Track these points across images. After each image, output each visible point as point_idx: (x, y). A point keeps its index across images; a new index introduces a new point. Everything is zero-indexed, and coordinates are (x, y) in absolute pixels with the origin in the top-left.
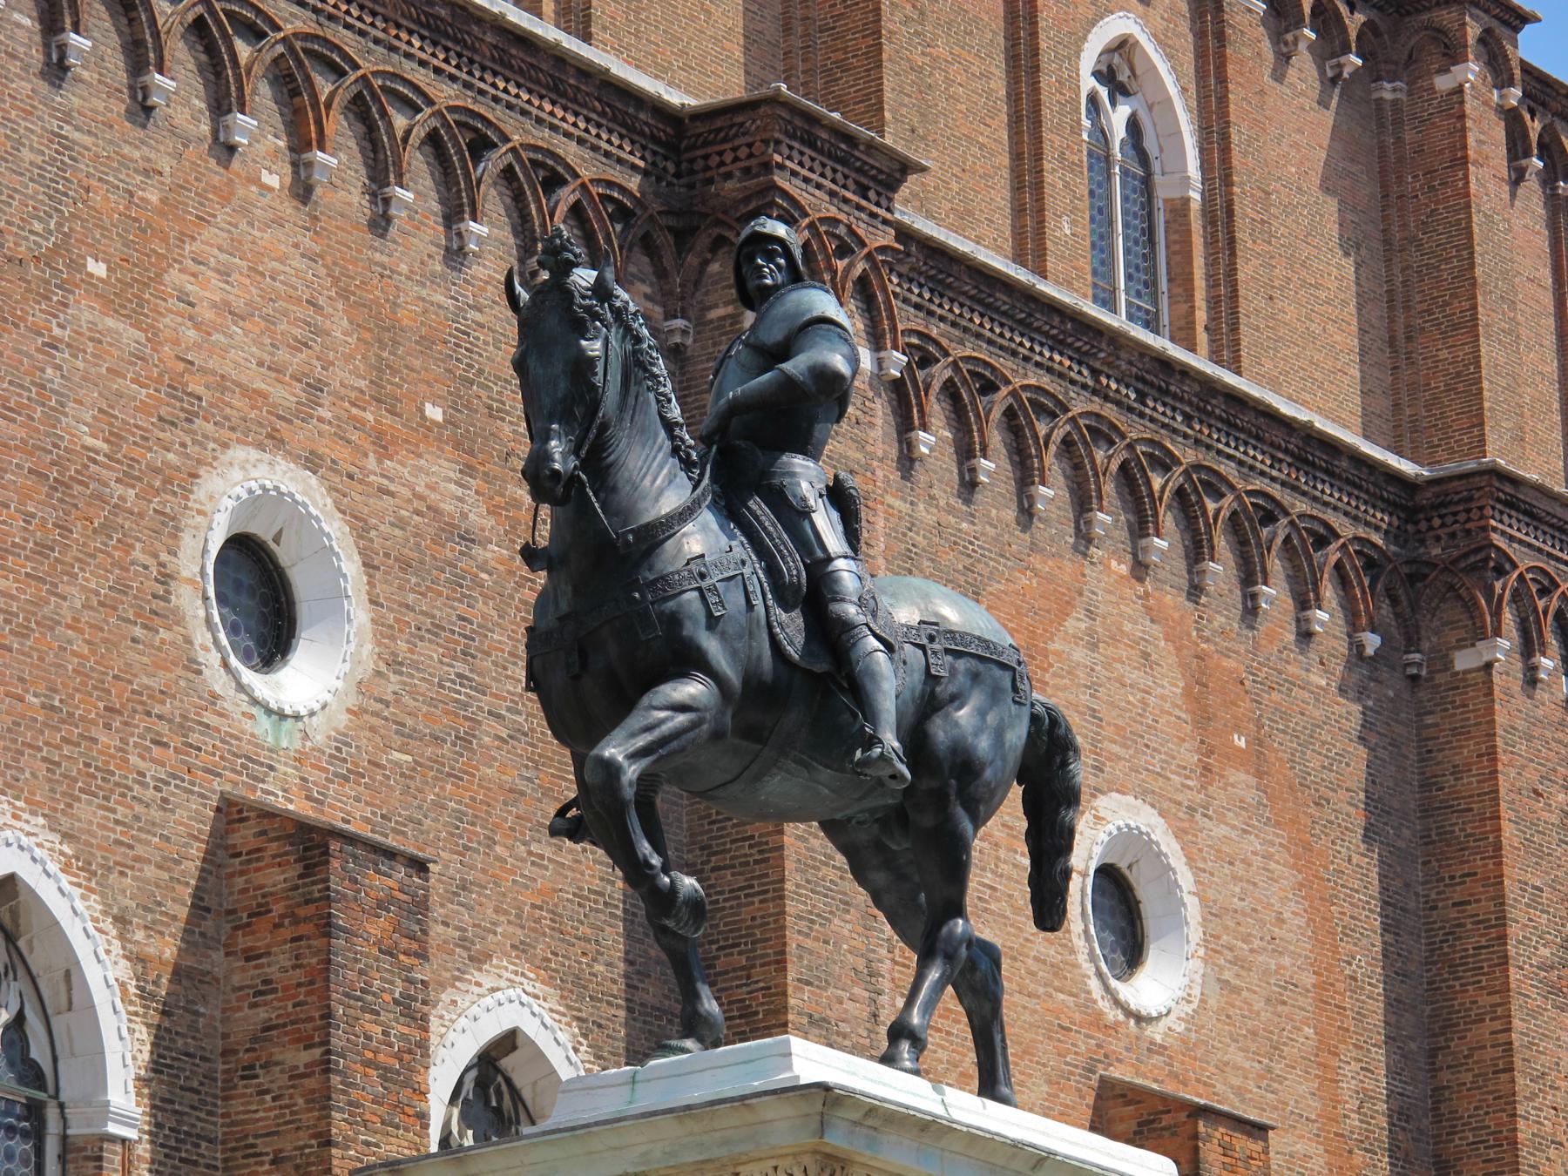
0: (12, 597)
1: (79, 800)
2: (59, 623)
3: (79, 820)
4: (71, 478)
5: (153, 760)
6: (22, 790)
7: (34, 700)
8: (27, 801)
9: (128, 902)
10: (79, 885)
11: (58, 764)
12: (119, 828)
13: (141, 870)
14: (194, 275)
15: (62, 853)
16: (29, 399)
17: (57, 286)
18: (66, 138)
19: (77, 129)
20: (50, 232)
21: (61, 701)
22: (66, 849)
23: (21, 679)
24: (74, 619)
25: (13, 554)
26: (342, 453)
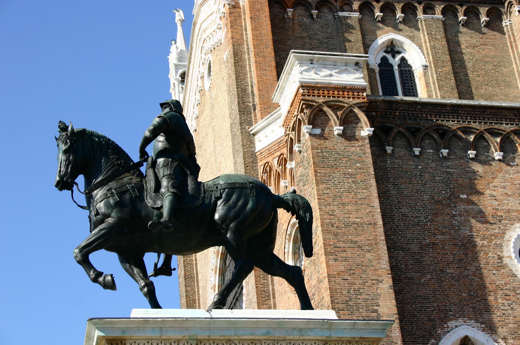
0: (453, 273)
1: (484, 314)
2: (469, 275)
3: (485, 318)
4: (466, 243)
5: (506, 300)
6: (466, 316)
7: (465, 294)
8: (467, 318)
9: (505, 334)
10: (489, 333)
11: (476, 307)
12: (499, 318)
13: (508, 326)
14: (494, 190)
15: (481, 327)
16: (449, 229)
17: (452, 203)
18: (448, 172)
19: (451, 169)
20: (448, 192)
21: (473, 293)
22: (482, 326)
23: (460, 291)
24: (473, 274)
25: (451, 264)
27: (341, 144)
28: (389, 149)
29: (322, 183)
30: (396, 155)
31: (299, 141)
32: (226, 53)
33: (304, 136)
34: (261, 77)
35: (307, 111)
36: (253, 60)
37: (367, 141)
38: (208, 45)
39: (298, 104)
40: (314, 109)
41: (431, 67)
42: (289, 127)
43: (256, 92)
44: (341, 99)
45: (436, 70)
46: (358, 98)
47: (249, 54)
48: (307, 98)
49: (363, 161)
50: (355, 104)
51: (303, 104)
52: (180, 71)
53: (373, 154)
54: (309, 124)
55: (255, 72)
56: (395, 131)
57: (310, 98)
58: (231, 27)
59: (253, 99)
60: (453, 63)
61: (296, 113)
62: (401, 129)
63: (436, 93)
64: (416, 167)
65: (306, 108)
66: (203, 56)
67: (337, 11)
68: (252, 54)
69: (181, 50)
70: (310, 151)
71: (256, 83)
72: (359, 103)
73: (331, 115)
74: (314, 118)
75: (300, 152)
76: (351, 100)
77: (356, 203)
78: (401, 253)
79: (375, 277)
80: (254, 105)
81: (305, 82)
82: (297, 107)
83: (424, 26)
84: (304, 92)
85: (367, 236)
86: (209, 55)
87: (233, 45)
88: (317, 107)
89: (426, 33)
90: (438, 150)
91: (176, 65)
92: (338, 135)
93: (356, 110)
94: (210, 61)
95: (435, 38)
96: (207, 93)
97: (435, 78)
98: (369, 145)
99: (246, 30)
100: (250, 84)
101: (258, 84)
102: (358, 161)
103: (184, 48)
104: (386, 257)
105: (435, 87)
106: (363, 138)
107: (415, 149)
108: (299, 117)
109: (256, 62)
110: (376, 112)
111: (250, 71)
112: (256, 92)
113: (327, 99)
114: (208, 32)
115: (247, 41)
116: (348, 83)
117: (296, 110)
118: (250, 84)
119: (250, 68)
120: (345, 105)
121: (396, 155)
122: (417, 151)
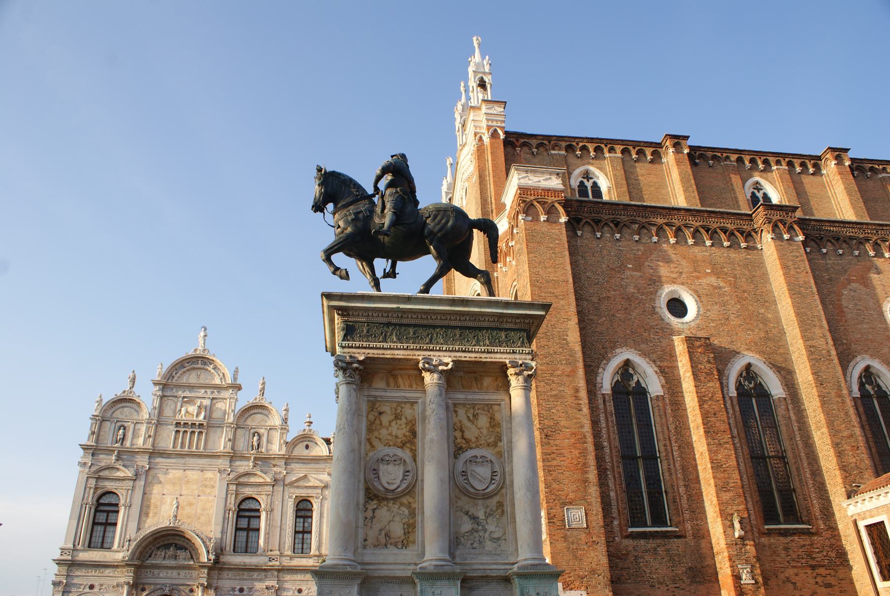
26: (689, 281)
27: (545, 228)
28: (579, 233)
29: (531, 253)
31: (517, 226)
32: (475, 178)
33: (520, 222)
36: (492, 180)
37: (564, 226)
38: (466, 176)
44: (546, 197)
47: (489, 176)
48: (522, 196)
49: (561, 239)
50: (555, 201)
53: (567, 237)
54: (523, 213)
56: (584, 221)
57: (525, 196)
58: (478, 159)
59: (491, 206)
62: (588, 220)
64: (598, 246)
65: (522, 203)
67: (550, 150)
68: (491, 176)
70: (524, 232)
75: (517, 233)
77: (555, 267)
80: (492, 210)
87: (479, 171)
90: (613, 235)
92: (544, 221)
93: (557, 205)
99: (488, 161)
107: (597, 233)
108: (517, 209)
109: (494, 181)
110: (571, 208)
113: (536, 197)
114: (465, 168)
115: (488, 168)
119: (490, 185)
122: (599, 235)
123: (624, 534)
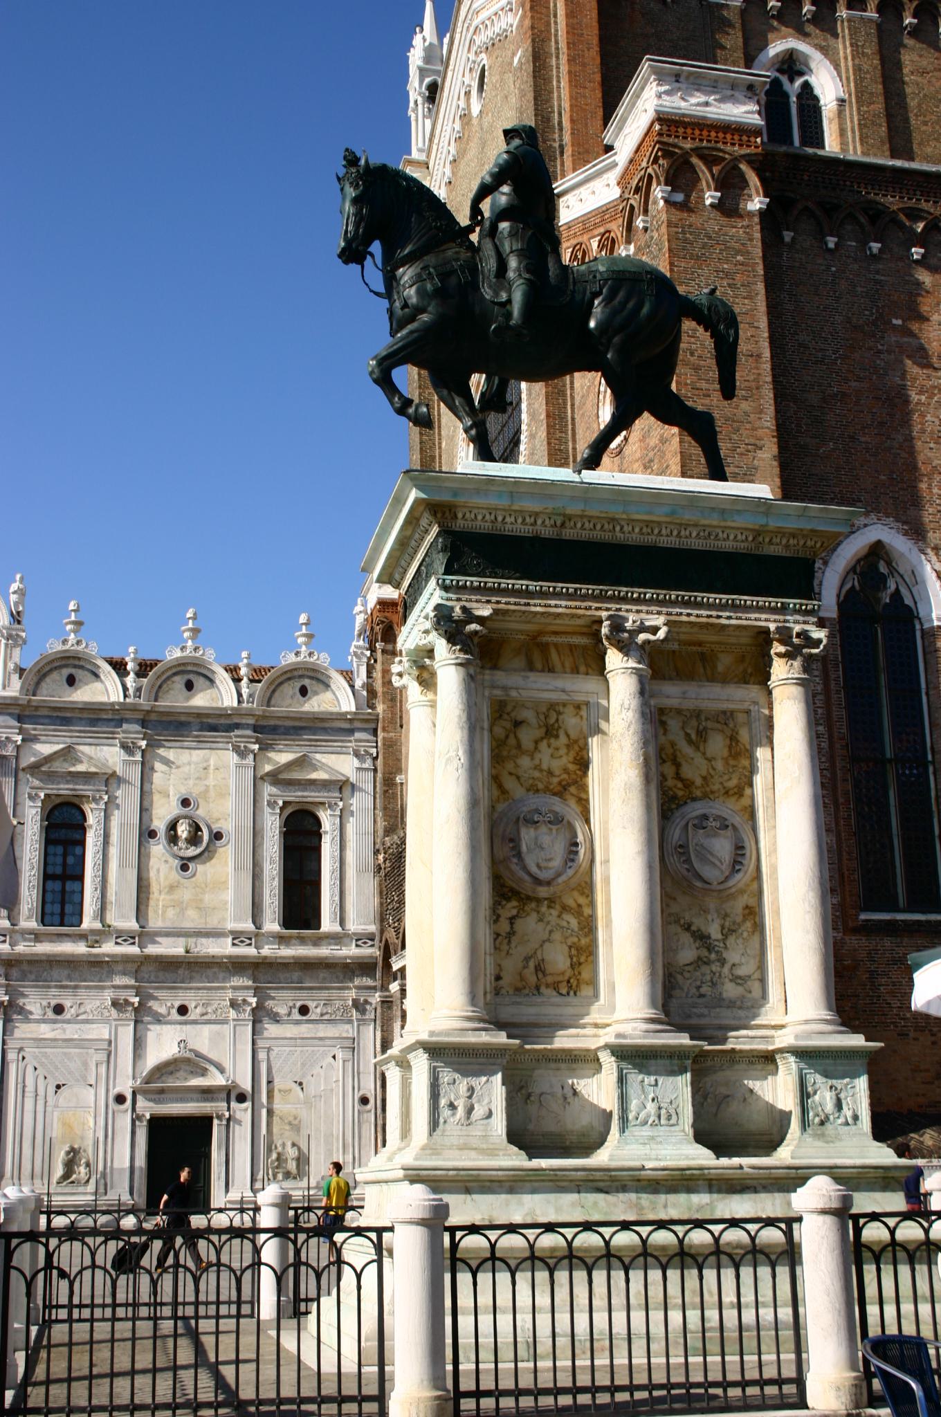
27: (714, 223)
28: (788, 236)
30: (798, 247)
32: (520, 56)
33: (655, 202)
34: (576, 99)
35: (665, 162)
36: (564, 68)
37: (756, 220)
38: (481, 39)
39: (650, 149)
40: (676, 160)
41: (851, 102)
42: (629, 186)
43: (566, 123)
44: (720, 145)
45: (858, 109)
46: (748, 146)
47: (557, 57)
48: (665, 139)
49: (748, 253)
50: (743, 156)
51: (659, 149)
52: (427, 80)
54: (666, 184)
55: (567, 89)
57: (671, 140)
58: (532, 8)
59: (561, 136)
60: (886, 99)
61: (644, 164)
63: (855, 148)
65: (664, 157)
66: (472, 56)
68: (564, 59)
69: (431, 44)
71: (568, 109)
72: (748, 155)
73: (703, 171)
74: (675, 176)
76: (736, 148)
78: (792, 405)
79: (752, 441)
80: (562, 147)
81: (663, 113)
82: (648, 154)
83: (847, 31)
84: (661, 129)
85: (745, 374)
86: (483, 55)
87: (533, 41)
88: (682, 156)
89: (848, 44)
91: (421, 70)
92: (712, 205)
94: (484, 66)
95: (863, 52)
96: (475, 122)
97: (856, 122)
98: (758, 227)
99: (555, 16)
100: (556, 110)
101: (571, 110)
102: (738, 252)
103: (435, 42)
104: (771, 410)
105: (854, 138)
106: (750, 214)
108: (650, 170)
109: (570, 72)
111: (559, 87)
112: (566, 123)
113: (697, 144)
114: (483, 15)
115: (556, 35)
116: (733, 119)
117: (645, 160)
118: (556, 110)
119: (559, 81)
120: (727, 156)
121: (798, 247)
123: (851, 924)
